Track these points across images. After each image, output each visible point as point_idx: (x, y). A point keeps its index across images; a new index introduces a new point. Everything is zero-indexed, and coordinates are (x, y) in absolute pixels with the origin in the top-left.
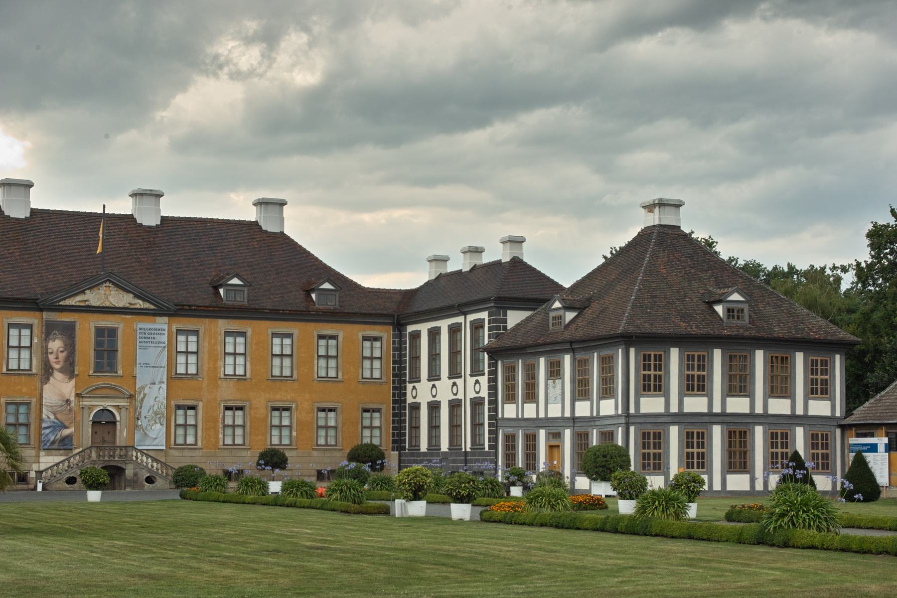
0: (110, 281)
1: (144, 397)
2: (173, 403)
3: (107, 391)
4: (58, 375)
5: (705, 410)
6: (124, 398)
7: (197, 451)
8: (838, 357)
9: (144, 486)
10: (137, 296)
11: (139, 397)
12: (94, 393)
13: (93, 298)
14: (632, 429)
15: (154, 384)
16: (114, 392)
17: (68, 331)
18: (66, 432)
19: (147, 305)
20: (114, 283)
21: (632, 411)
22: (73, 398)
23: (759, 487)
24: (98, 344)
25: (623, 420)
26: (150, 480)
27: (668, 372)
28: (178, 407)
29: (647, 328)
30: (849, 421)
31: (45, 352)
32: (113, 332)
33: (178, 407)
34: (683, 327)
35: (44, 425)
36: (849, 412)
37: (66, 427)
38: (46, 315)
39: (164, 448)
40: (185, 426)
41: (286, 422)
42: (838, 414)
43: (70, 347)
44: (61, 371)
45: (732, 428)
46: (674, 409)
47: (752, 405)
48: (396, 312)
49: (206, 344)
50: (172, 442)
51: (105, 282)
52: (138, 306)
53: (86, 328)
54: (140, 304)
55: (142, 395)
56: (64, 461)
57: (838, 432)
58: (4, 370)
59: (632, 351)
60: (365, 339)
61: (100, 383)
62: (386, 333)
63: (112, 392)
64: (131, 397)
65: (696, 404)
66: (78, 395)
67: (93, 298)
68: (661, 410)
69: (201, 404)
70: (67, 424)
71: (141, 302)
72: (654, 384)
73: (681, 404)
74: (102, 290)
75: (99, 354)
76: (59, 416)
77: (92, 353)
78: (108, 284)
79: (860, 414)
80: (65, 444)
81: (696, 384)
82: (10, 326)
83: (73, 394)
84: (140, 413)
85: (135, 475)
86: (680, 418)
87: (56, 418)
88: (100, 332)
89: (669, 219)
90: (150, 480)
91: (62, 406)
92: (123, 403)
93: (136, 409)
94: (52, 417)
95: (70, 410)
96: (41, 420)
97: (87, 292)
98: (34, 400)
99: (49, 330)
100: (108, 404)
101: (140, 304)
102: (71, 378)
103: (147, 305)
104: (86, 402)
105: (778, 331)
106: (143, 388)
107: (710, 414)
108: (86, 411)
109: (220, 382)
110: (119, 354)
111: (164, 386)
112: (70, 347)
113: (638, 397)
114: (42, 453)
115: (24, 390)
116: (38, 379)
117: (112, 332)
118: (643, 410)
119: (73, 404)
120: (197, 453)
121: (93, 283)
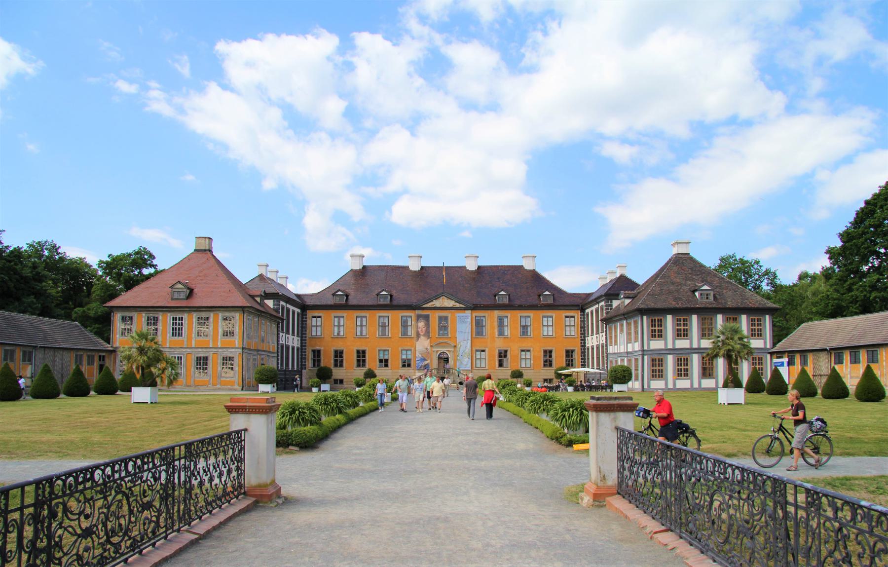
2: (474, 349)
4: (422, 337)
5: (688, 347)
8: (767, 317)
11: (458, 346)
13: (437, 303)
14: (646, 357)
17: (427, 318)
18: (426, 362)
21: (645, 348)
23: (696, 385)
27: (666, 328)
28: (477, 351)
29: (652, 305)
30: (773, 350)
31: (417, 327)
32: (446, 318)
33: (477, 351)
34: (674, 304)
36: (774, 345)
38: (417, 312)
40: (480, 359)
41: (528, 357)
42: (768, 347)
43: (428, 325)
44: (424, 335)
46: (670, 346)
47: (691, 343)
48: (579, 303)
54: (458, 305)
57: (769, 356)
59: (645, 318)
60: (566, 317)
61: (441, 341)
62: (577, 314)
64: (455, 347)
65: (683, 344)
67: (437, 303)
68: (663, 347)
69: (487, 350)
72: (657, 334)
73: (674, 343)
74: (441, 299)
77: (437, 328)
79: (779, 347)
81: (683, 333)
82: (543, 317)
86: (673, 351)
88: (440, 318)
89: (682, 250)
92: (451, 349)
99: (419, 317)
101: (458, 305)
104: (435, 349)
105: (730, 304)
107: (691, 349)
112: (428, 325)
113: (648, 340)
117: (446, 318)
118: (652, 348)
121: (437, 297)
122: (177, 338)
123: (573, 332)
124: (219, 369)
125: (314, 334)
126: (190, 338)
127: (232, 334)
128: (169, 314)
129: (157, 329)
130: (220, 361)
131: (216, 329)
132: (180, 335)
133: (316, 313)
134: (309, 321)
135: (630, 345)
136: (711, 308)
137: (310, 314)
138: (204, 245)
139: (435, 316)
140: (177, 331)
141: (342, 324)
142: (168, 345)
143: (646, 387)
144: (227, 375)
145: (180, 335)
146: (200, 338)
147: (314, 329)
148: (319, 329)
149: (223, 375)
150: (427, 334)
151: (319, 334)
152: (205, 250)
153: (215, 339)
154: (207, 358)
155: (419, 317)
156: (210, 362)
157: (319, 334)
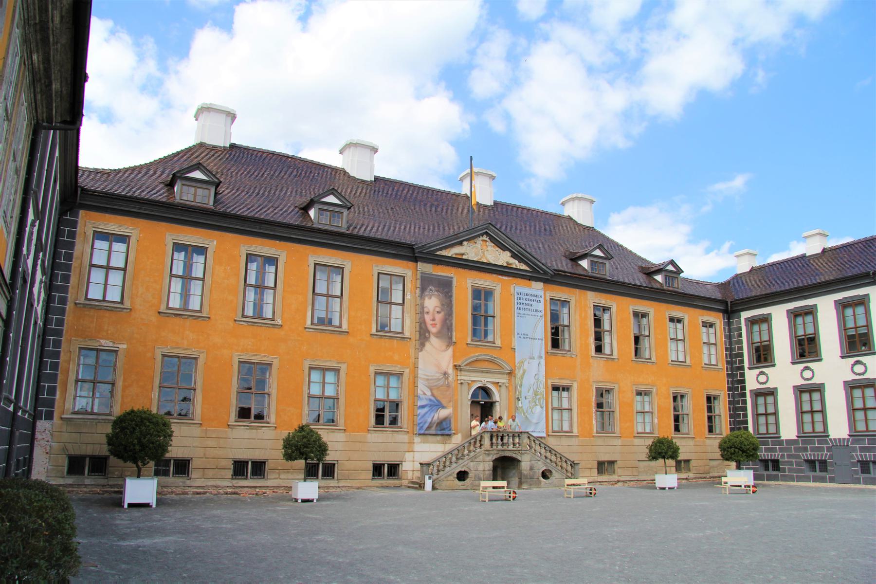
0: (486, 233)
1: (524, 373)
2: (550, 384)
3: (486, 365)
4: (434, 340)
6: (503, 373)
7: (574, 439)
9: (540, 482)
10: (514, 256)
11: (519, 374)
12: (474, 365)
15: (533, 358)
16: (491, 364)
17: (445, 287)
18: (443, 413)
19: (524, 267)
20: (493, 240)
22: (450, 371)
26: (545, 475)
31: (421, 311)
35: (420, 403)
37: (443, 407)
38: (423, 267)
39: (544, 435)
44: (438, 335)
49: (577, 317)
50: (550, 428)
51: (482, 235)
54: (515, 264)
55: (521, 371)
62: (718, 319)
63: (491, 366)
64: (511, 374)
66: (456, 367)
67: (472, 251)
69: (575, 386)
70: (444, 403)
71: (517, 262)
76: (435, 392)
78: (485, 238)
80: (443, 429)
83: (451, 366)
84: (520, 393)
85: (531, 469)
87: (433, 395)
88: (477, 293)
90: (545, 475)
91: (439, 380)
92: (503, 380)
93: (516, 387)
94: (429, 393)
95: (448, 386)
96: (416, 396)
97: (465, 243)
98: (407, 371)
99: (426, 282)
100: (485, 380)
101: (515, 264)
102: (448, 346)
103: (524, 267)
104: (465, 377)
106: (522, 363)
108: (465, 387)
109: (591, 360)
111: (543, 362)
114: (417, 439)
115: (396, 357)
116: (412, 346)
119: (450, 379)
120: (574, 441)
121: (471, 236)
123: (716, 356)
125: (95, 293)
133: (113, 224)
134: (80, 248)
137: (88, 222)
139: (464, 283)
141: (198, 272)
147: (97, 276)
148: (116, 278)
150: (447, 331)
151: (114, 295)
155: (426, 282)
157: (114, 295)
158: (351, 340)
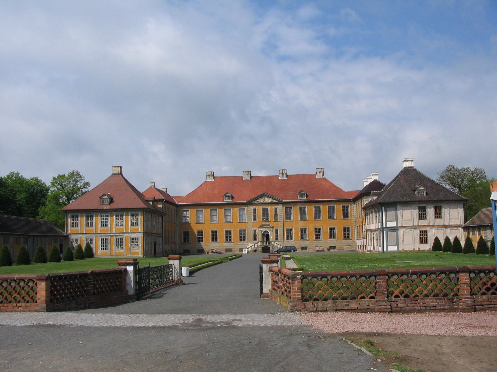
2: (285, 228)
12: (262, 226)
13: (262, 201)
14: (385, 232)
19: (276, 201)
21: (384, 226)
24: (263, 213)
25: (381, 229)
32: (267, 209)
42: (462, 224)
45: (421, 229)
52: (274, 202)
53: (259, 209)
54: (274, 201)
56: (253, 246)
58: (238, 221)
61: (264, 223)
67: (262, 201)
68: (395, 225)
75: (263, 216)
100: (266, 229)
101: (274, 201)
103: (276, 201)
109: (299, 222)
110: (269, 216)
118: (388, 226)
122: (104, 228)
124: (130, 245)
126: (112, 227)
127: (137, 224)
128: (99, 214)
129: (92, 223)
130: (130, 240)
131: (127, 221)
132: (106, 225)
135: (376, 224)
136: (425, 201)
138: (117, 171)
139: (259, 209)
140: (104, 224)
142: (99, 232)
143: (385, 250)
144: (135, 249)
145: (106, 225)
146: (118, 227)
149: (132, 248)
152: (118, 174)
153: (127, 228)
154: (122, 239)
156: (124, 241)
158: (233, 224)
